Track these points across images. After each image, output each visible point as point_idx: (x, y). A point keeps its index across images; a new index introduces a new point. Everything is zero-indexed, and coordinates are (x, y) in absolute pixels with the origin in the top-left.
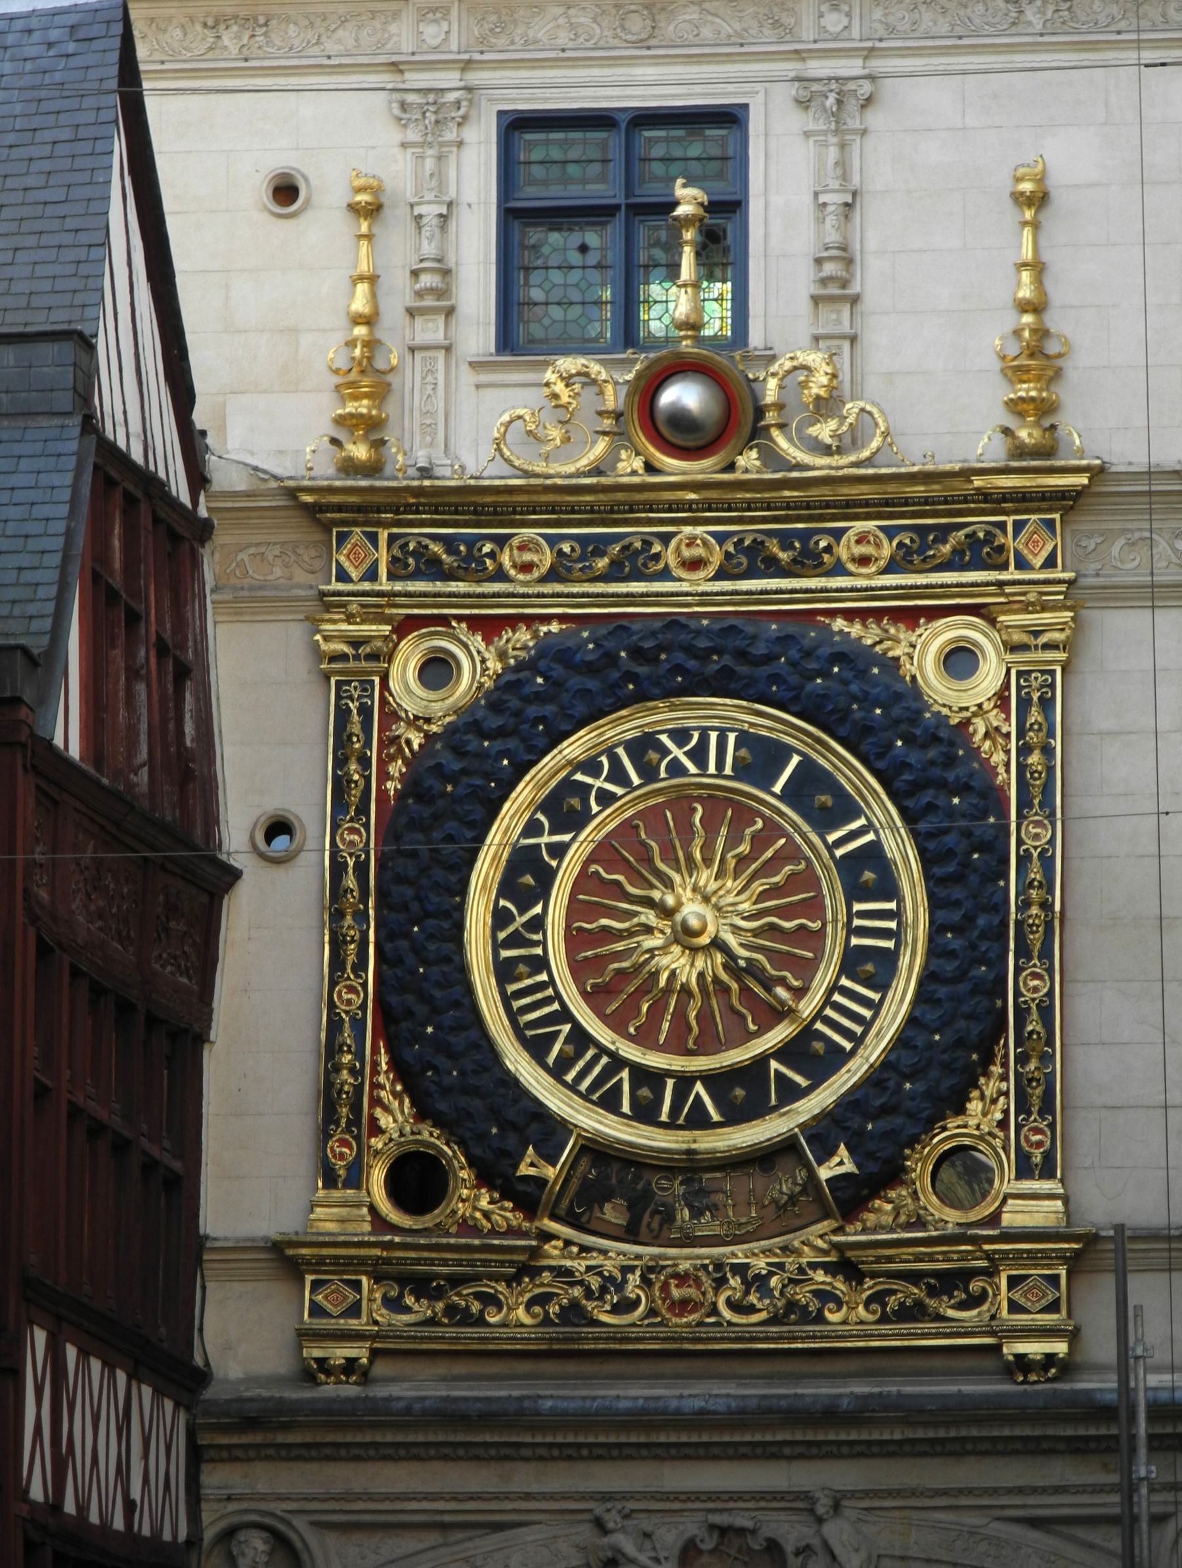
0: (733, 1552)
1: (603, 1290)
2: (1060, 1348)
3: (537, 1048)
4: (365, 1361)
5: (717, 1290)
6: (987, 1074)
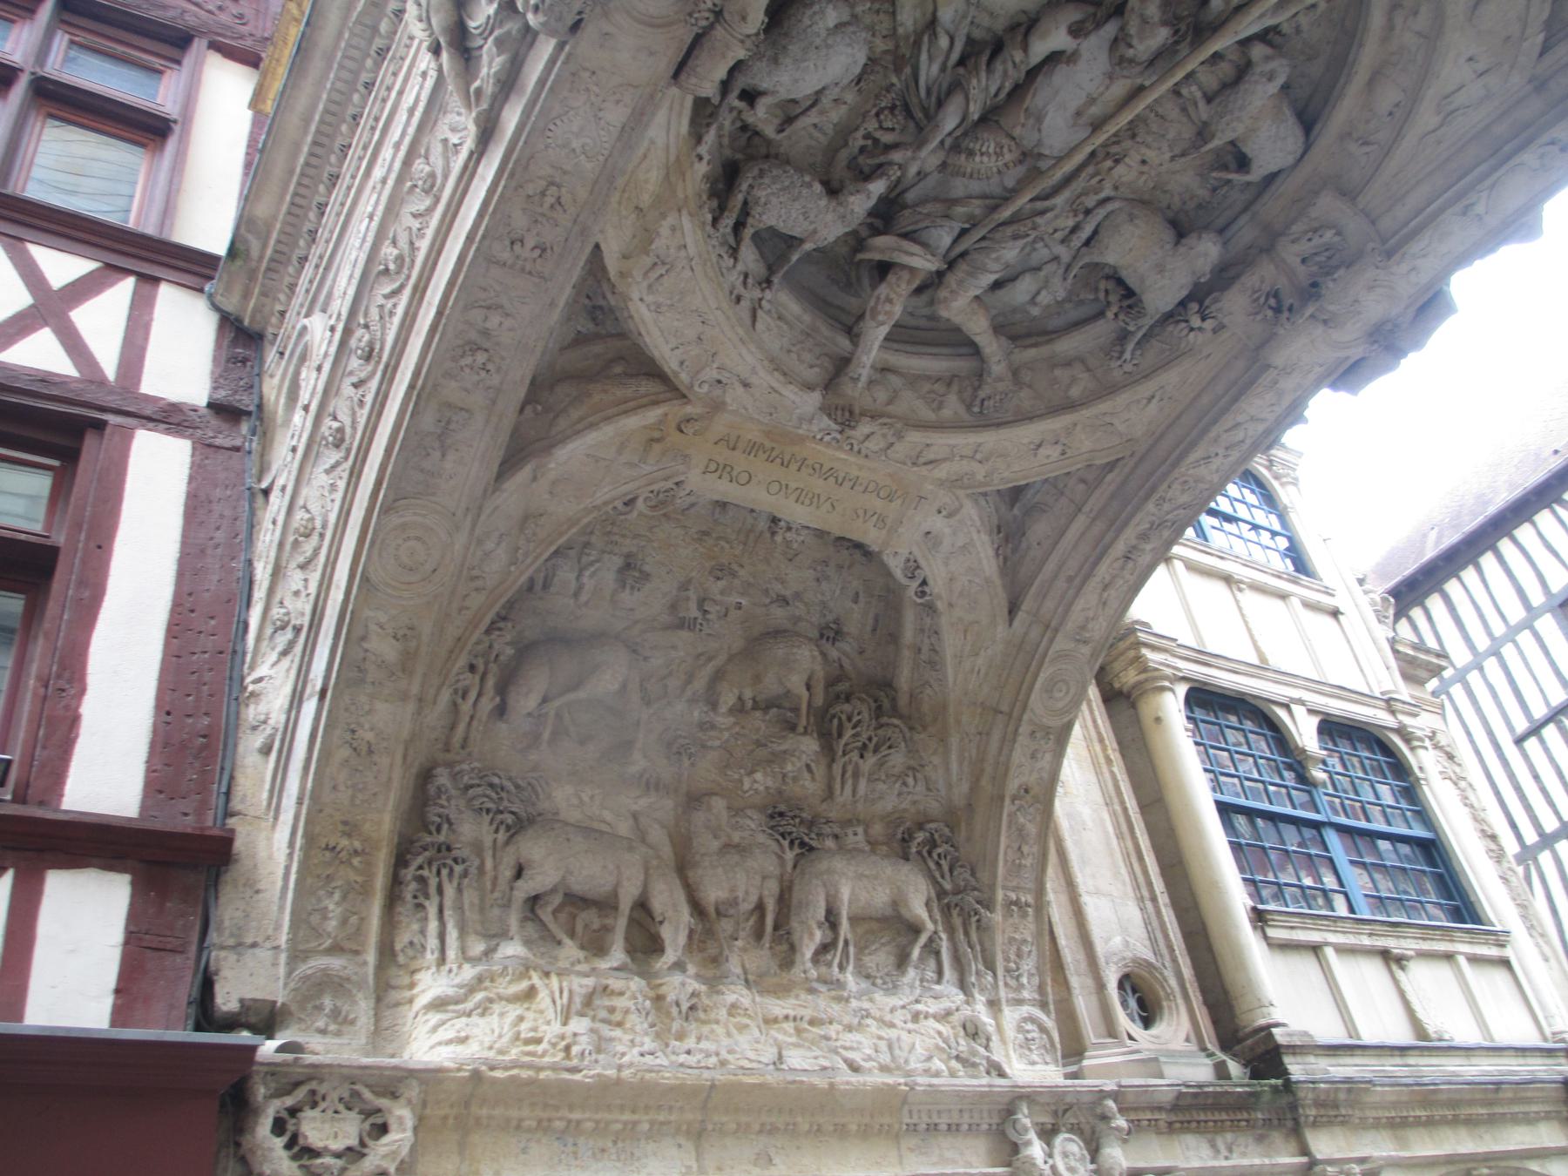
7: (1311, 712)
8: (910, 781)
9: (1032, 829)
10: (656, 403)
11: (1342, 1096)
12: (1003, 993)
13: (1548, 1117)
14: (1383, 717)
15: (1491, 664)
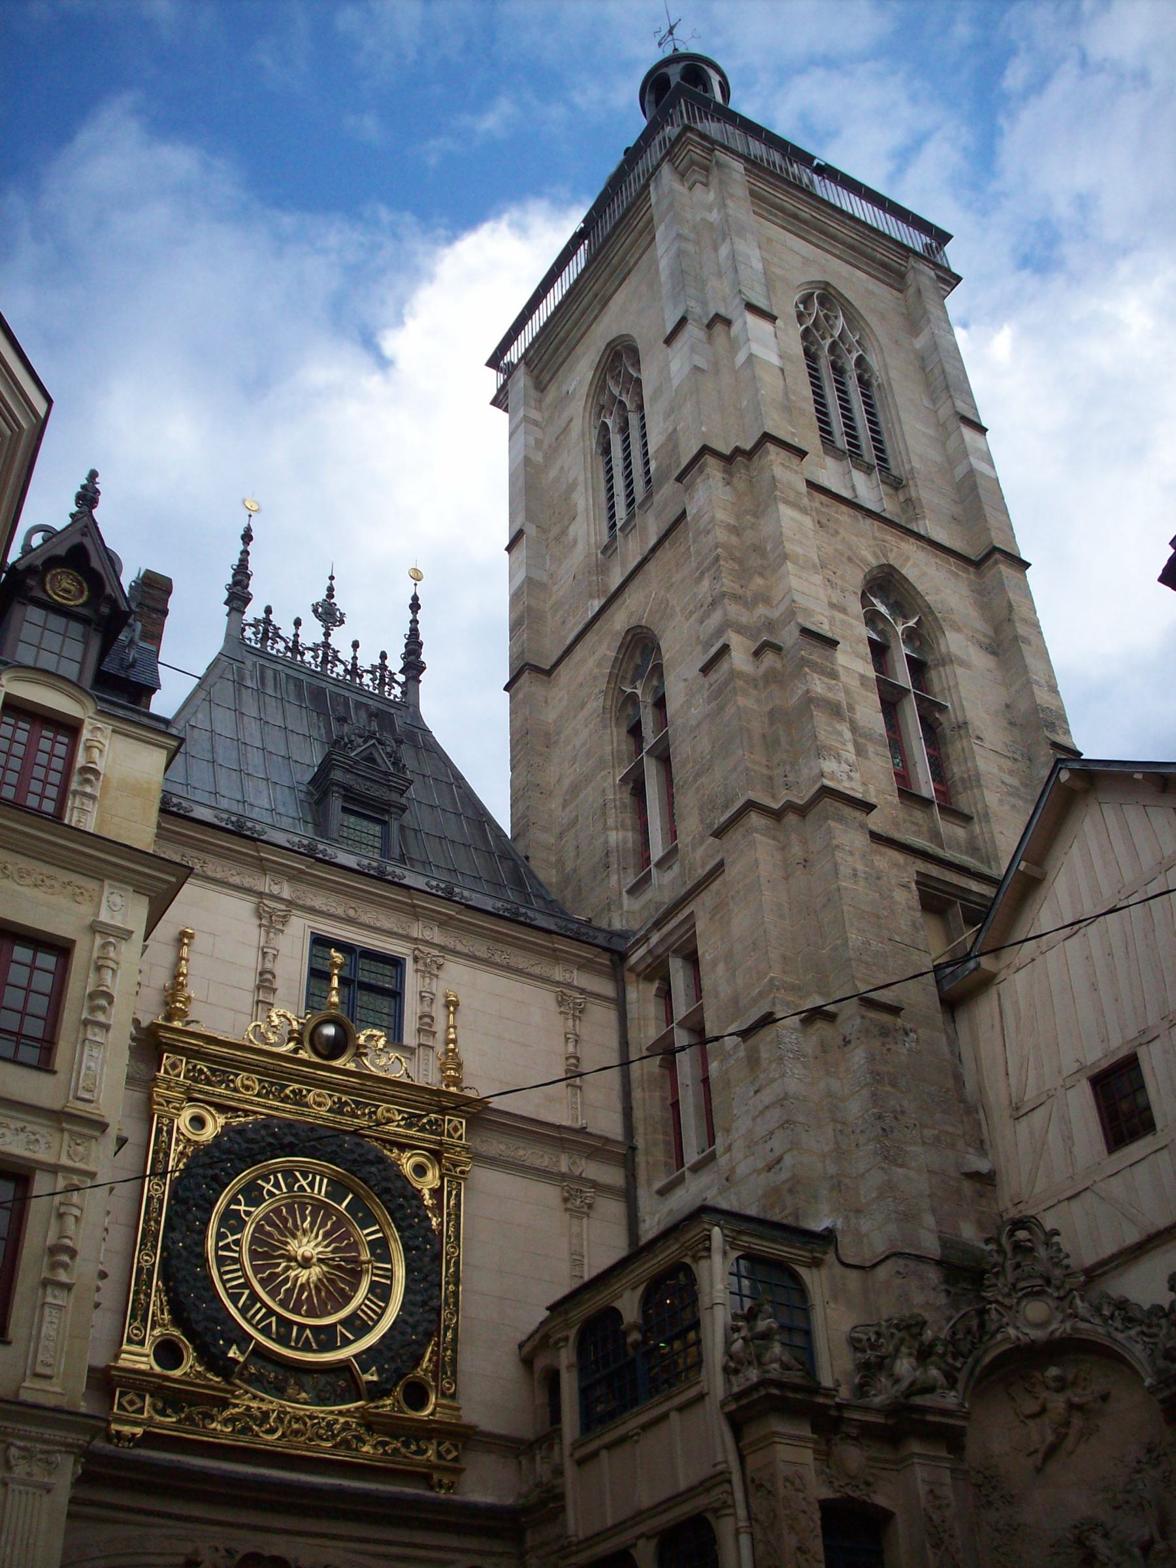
3: (234, 1298)
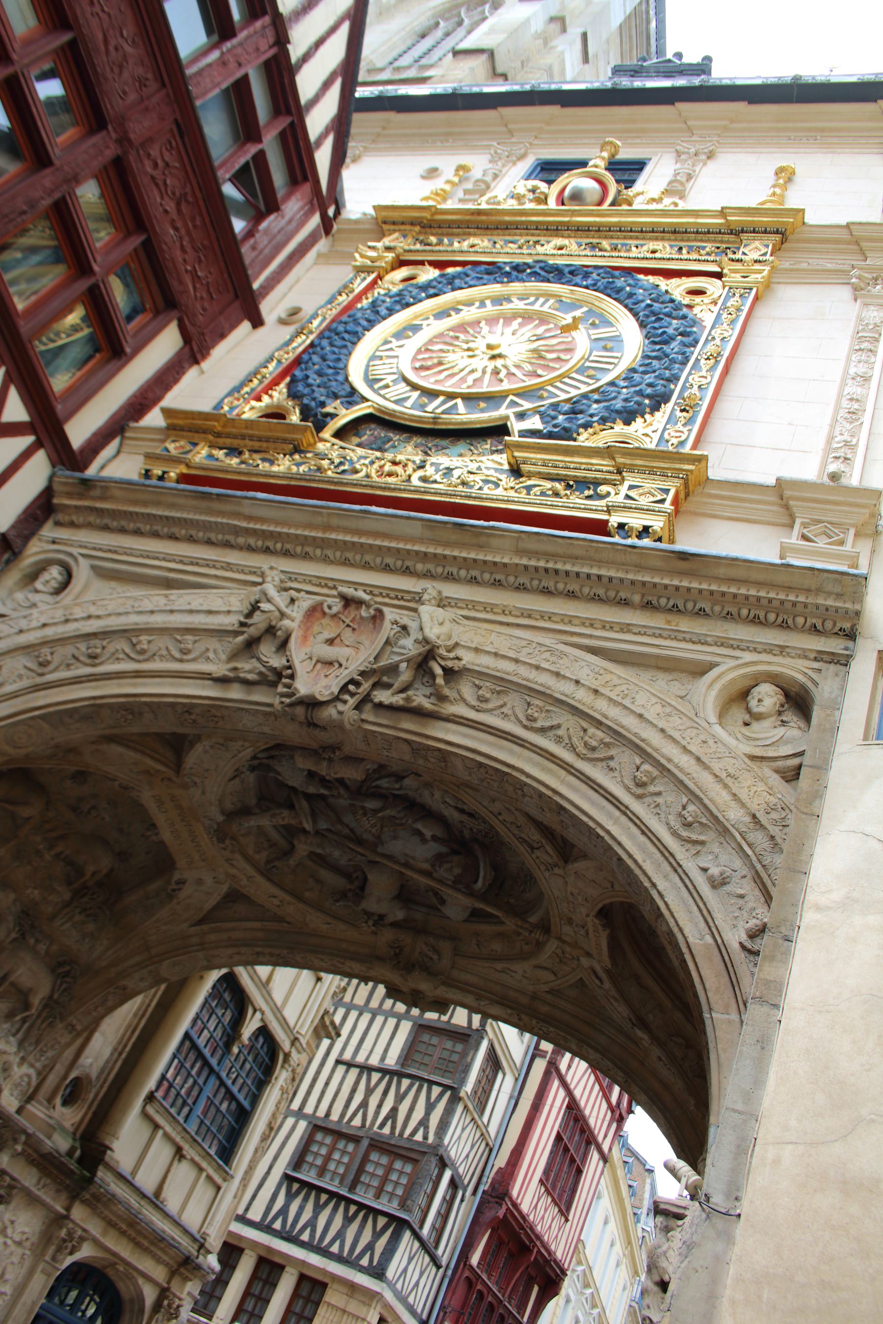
0: (348, 621)
1: (341, 463)
2: (657, 524)
3: (371, 382)
4: (172, 475)
5: (414, 471)
6: (652, 413)
7: (262, 1020)
8: (87, 940)
9: (110, 1004)
10: (166, 765)
11: (105, 1199)
12: (31, 1058)
13: (167, 1265)
14: (286, 1045)
15: (367, 1017)
